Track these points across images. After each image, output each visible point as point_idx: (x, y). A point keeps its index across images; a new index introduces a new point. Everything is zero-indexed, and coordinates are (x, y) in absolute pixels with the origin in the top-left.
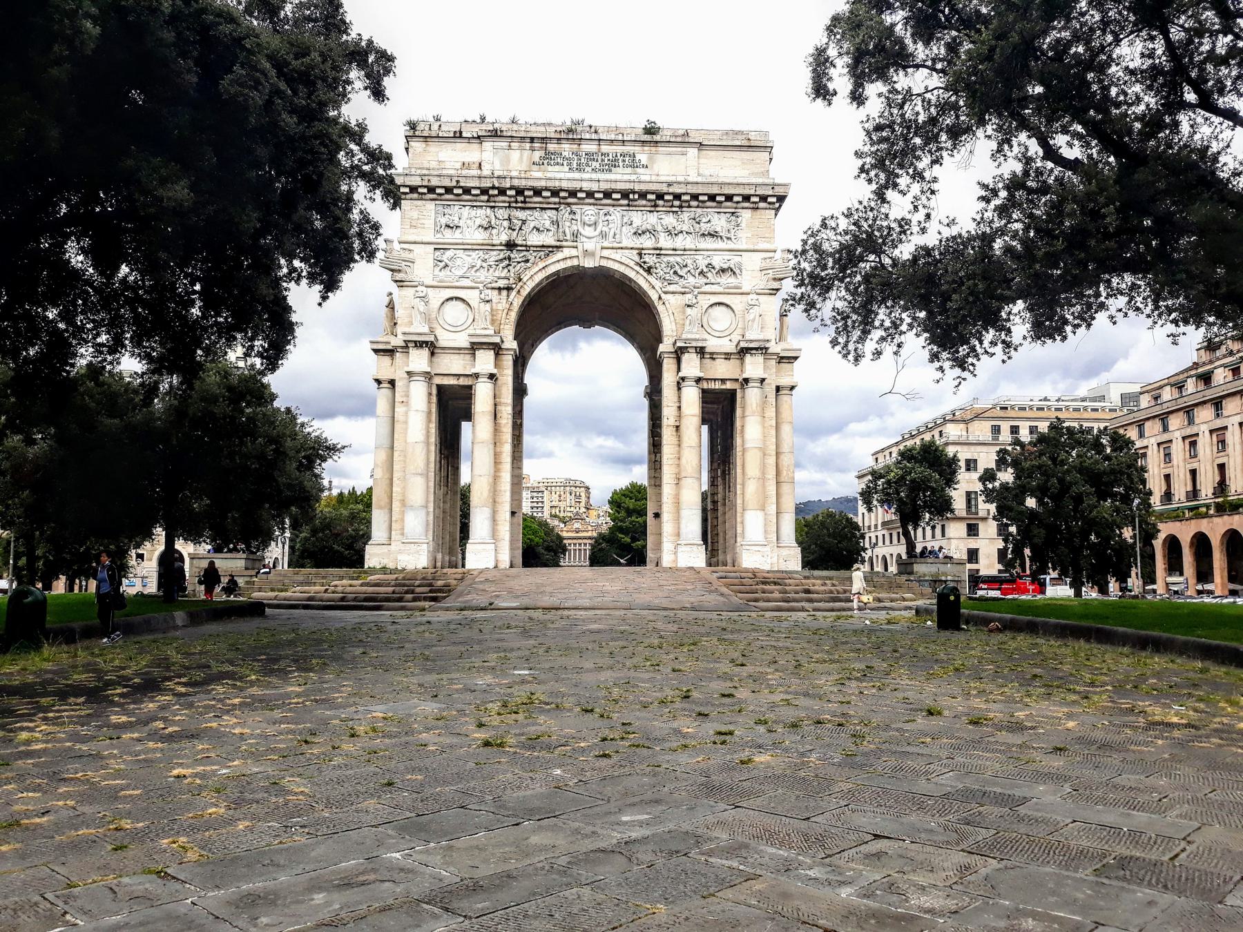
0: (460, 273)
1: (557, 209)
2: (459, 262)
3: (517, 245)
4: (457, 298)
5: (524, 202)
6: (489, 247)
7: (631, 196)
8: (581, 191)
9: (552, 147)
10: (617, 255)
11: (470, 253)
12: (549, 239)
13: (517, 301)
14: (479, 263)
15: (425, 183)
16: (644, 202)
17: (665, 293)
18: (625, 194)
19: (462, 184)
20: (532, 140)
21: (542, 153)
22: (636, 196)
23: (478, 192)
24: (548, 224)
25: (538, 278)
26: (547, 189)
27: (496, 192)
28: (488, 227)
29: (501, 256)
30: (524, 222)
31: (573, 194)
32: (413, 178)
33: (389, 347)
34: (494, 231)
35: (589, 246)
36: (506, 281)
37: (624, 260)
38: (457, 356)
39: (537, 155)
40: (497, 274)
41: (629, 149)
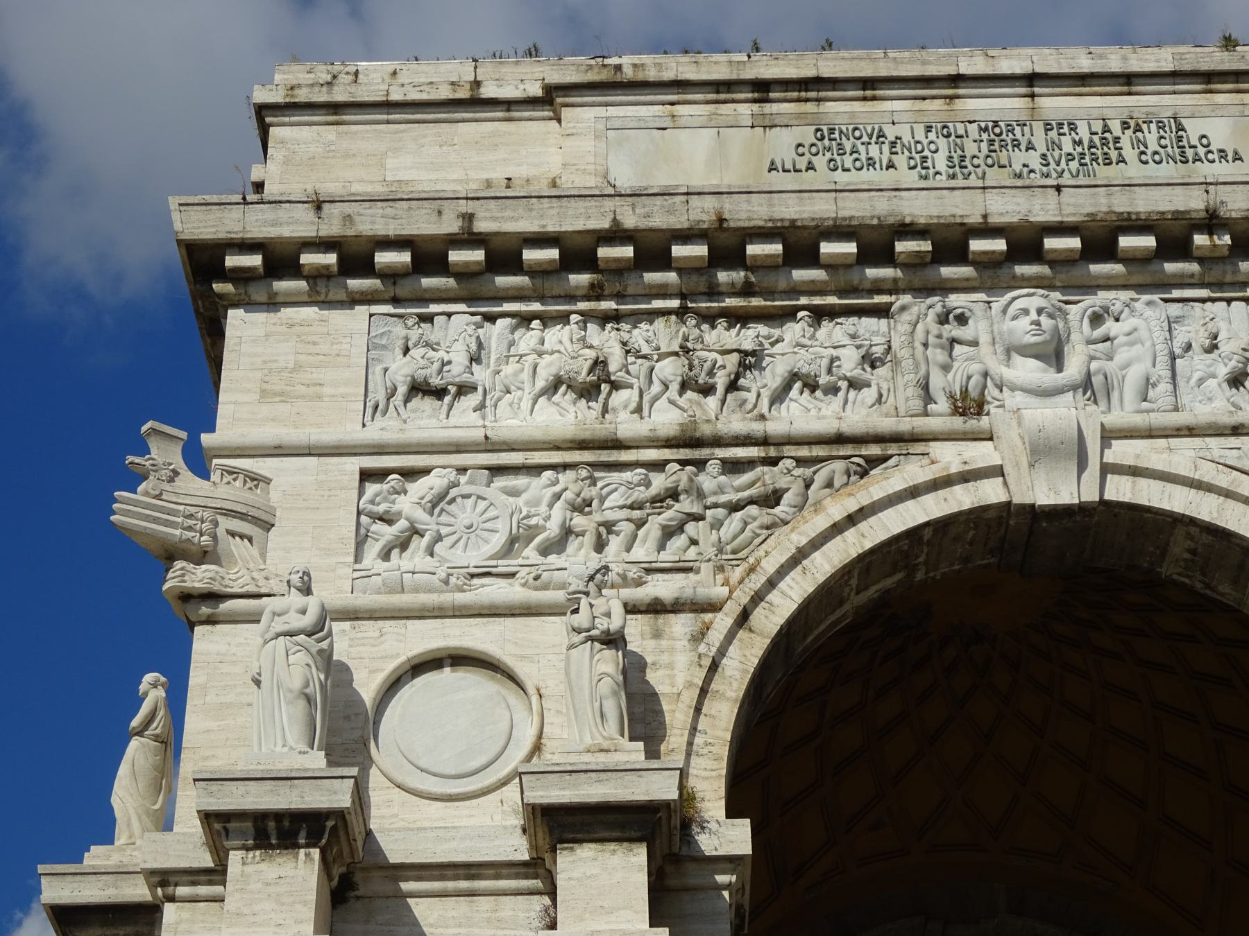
0: (475, 557)
1: (882, 312)
2: (464, 513)
3: (718, 441)
6: (604, 451)
9: (838, 110)
10: (1181, 456)
11: (520, 481)
12: (857, 414)
15: (331, 227)
18: (1174, 237)
19: (482, 226)
20: (762, 89)
24: (849, 361)
25: (825, 564)
26: (840, 231)
28: (595, 384)
29: (659, 482)
30: (750, 360)
31: (950, 243)
32: (284, 212)
33: (138, 892)
37: (1208, 473)
40: (642, 552)
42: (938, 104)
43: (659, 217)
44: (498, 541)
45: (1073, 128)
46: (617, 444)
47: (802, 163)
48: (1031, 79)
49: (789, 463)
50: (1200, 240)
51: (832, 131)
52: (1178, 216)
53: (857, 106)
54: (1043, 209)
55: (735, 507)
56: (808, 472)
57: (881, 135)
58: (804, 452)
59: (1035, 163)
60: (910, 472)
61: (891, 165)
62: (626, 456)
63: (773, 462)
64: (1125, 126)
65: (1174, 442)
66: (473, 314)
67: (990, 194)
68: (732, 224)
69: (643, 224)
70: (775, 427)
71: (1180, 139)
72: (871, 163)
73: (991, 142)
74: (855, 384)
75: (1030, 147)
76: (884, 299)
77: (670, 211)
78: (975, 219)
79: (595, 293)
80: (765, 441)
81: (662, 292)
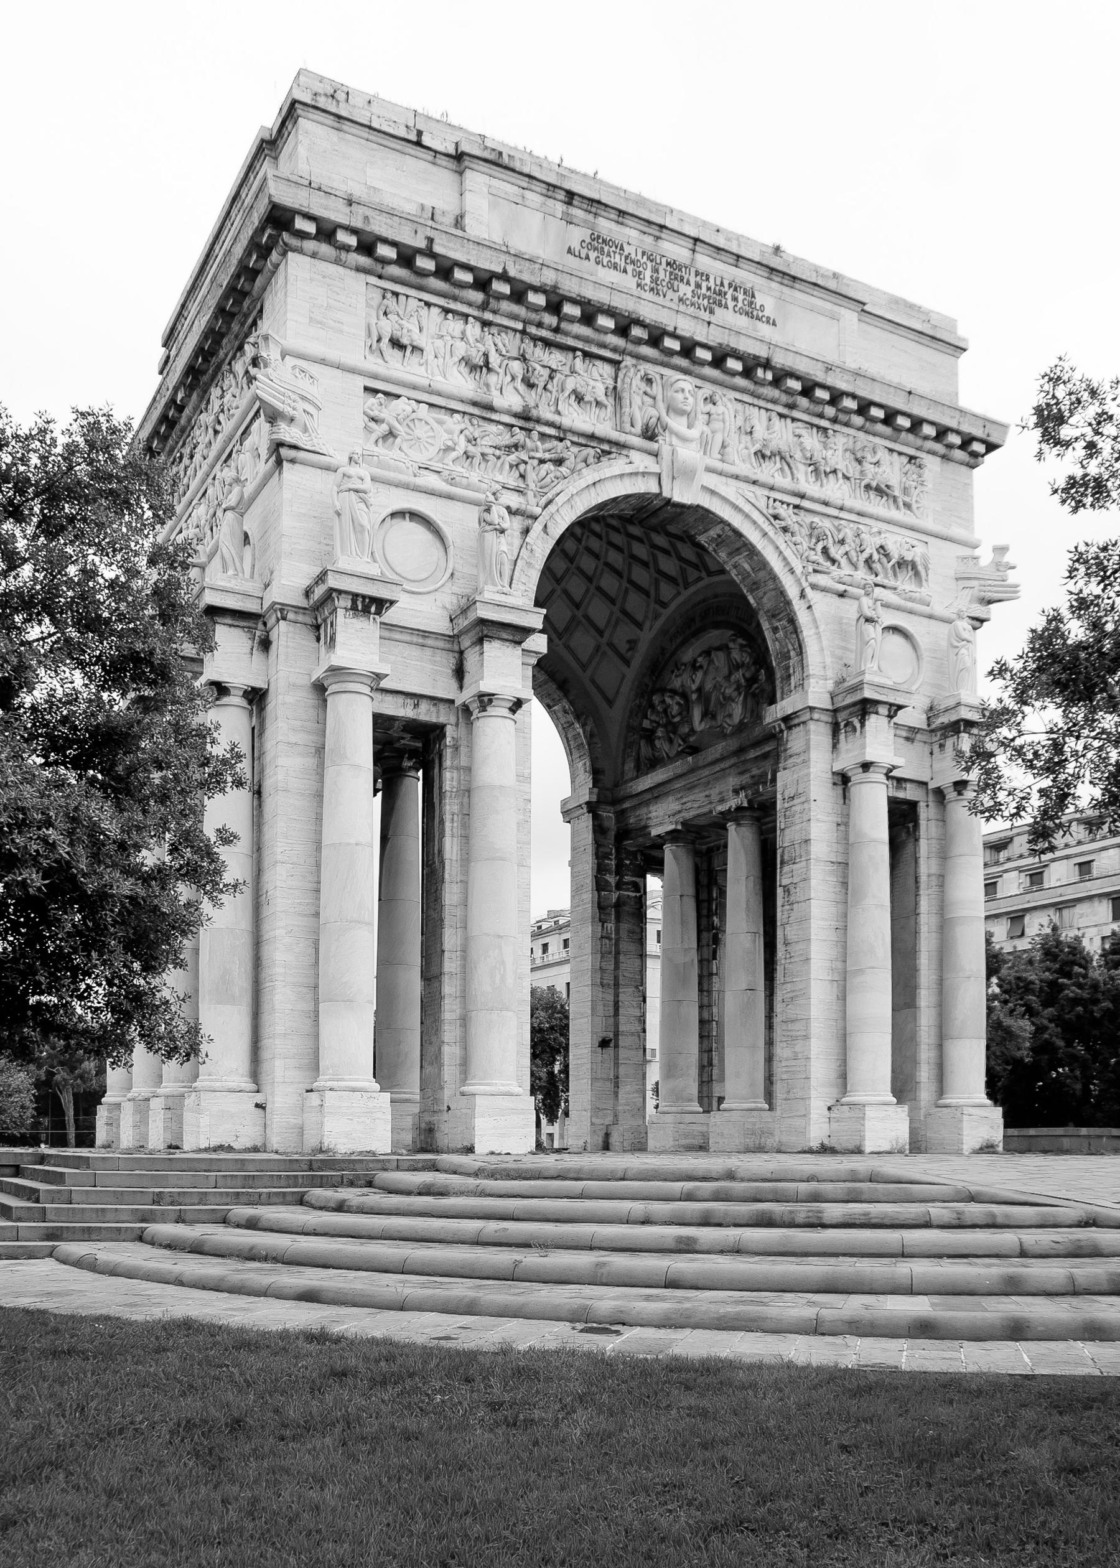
0: (422, 458)
1: (616, 364)
3: (538, 421)
4: (414, 516)
5: (557, 330)
7: (760, 372)
8: (674, 335)
9: (606, 226)
13: (541, 546)
14: (462, 445)
16: (775, 393)
17: (814, 587)
20: (571, 195)
21: (586, 234)
22: (769, 376)
23: (468, 278)
27: (505, 289)
31: (656, 338)
34: (492, 379)
35: (689, 454)
36: (521, 499)
37: (741, 503)
38: (415, 651)
39: (577, 236)
40: (500, 478)
41: (745, 276)
42: (650, 240)
43: (526, 277)
44: (433, 451)
45: (708, 279)
46: (490, 408)
47: (583, 256)
48: (696, 240)
49: (569, 443)
50: (760, 372)
51: (599, 237)
52: (756, 357)
53: (613, 225)
54: (700, 333)
55: (542, 461)
56: (575, 449)
57: (622, 249)
58: (575, 439)
59: (689, 295)
60: (617, 465)
61: (625, 271)
62: (495, 417)
63: (561, 440)
64: (730, 285)
65: (730, 480)
66: (420, 300)
67: (680, 316)
68: (561, 292)
69: (519, 276)
70: (566, 422)
71: (752, 303)
72: (615, 267)
73: (671, 273)
74: (598, 403)
75: (688, 283)
76: (616, 357)
77: (532, 273)
78: (670, 329)
79: (484, 307)
80: (559, 428)
81: (515, 317)
